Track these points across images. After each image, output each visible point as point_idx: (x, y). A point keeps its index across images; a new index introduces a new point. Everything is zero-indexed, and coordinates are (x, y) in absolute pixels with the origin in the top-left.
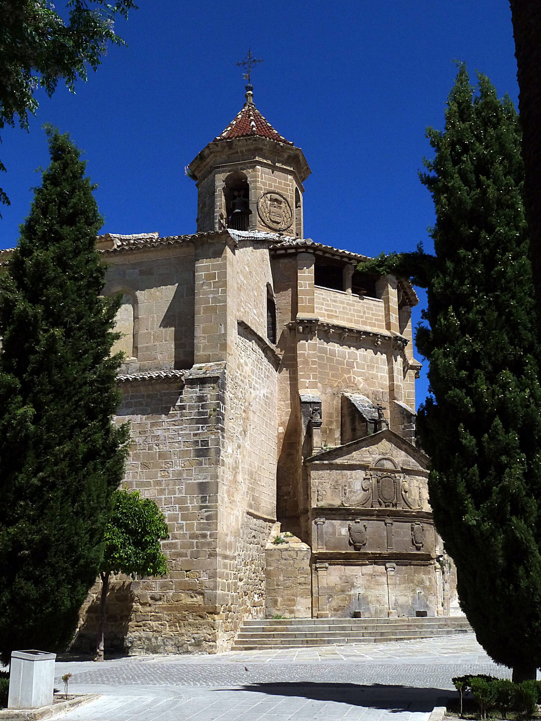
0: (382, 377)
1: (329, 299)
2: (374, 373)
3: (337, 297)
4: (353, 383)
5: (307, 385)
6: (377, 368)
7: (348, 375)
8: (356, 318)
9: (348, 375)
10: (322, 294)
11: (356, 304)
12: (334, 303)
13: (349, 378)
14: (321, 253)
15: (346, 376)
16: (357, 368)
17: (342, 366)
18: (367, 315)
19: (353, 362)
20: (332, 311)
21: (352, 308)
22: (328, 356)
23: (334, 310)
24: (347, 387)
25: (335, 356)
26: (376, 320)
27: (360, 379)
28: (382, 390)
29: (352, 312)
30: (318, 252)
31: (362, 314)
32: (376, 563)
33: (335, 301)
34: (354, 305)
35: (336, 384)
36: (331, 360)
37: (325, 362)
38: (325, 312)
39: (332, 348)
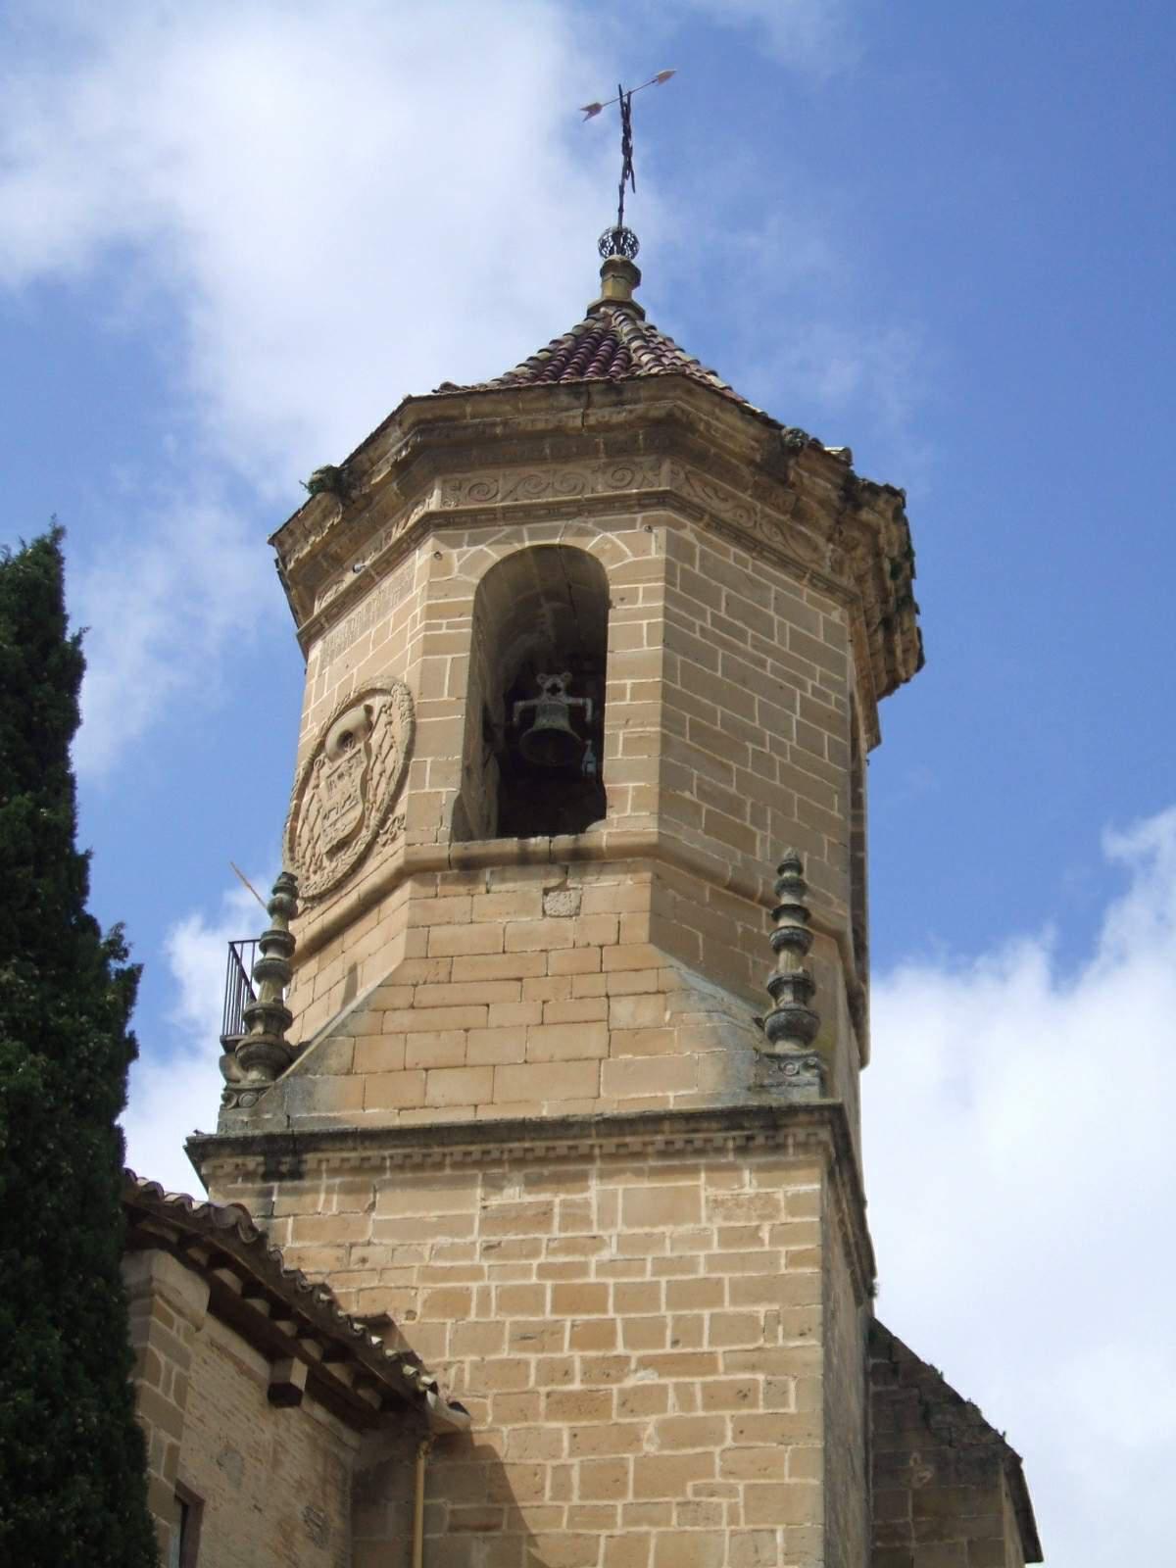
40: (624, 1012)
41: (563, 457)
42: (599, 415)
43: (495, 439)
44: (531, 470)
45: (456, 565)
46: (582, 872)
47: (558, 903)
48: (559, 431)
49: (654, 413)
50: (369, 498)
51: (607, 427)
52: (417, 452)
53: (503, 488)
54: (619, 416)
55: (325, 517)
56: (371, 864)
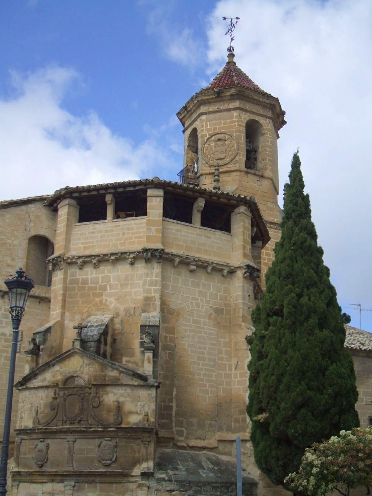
0: (136, 292)
1: (87, 233)
2: (128, 290)
3: (95, 229)
4: (105, 304)
5: (55, 317)
6: (131, 284)
7: (100, 299)
8: (114, 242)
9: (100, 299)
10: (80, 230)
11: (115, 228)
12: (92, 235)
13: (101, 302)
14: (77, 195)
15: (97, 300)
16: (110, 289)
17: (95, 291)
18: (126, 236)
19: (106, 285)
20: (89, 242)
21: (110, 234)
22: (80, 285)
23: (91, 241)
24: (99, 310)
25: (88, 284)
26: (136, 238)
27: (112, 299)
28: (135, 305)
29: (110, 238)
30: (75, 195)
31: (121, 236)
32: (53, 481)
33: (92, 233)
34: (112, 231)
35: (86, 309)
36: (83, 288)
37: (76, 291)
38: (82, 246)
39: (84, 277)
40: (269, 204)
41: (257, 104)
42: (265, 100)
43: (249, 98)
44: (252, 105)
45: (242, 118)
46: (263, 179)
47: (259, 183)
48: (258, 100)
49: (272, 103)
50: (222, 97)
51: (265, 102)
52: (237, 94)
53: (248, 106)
54: (267, 102)
55: (211, 95)
56: (229, 166)
